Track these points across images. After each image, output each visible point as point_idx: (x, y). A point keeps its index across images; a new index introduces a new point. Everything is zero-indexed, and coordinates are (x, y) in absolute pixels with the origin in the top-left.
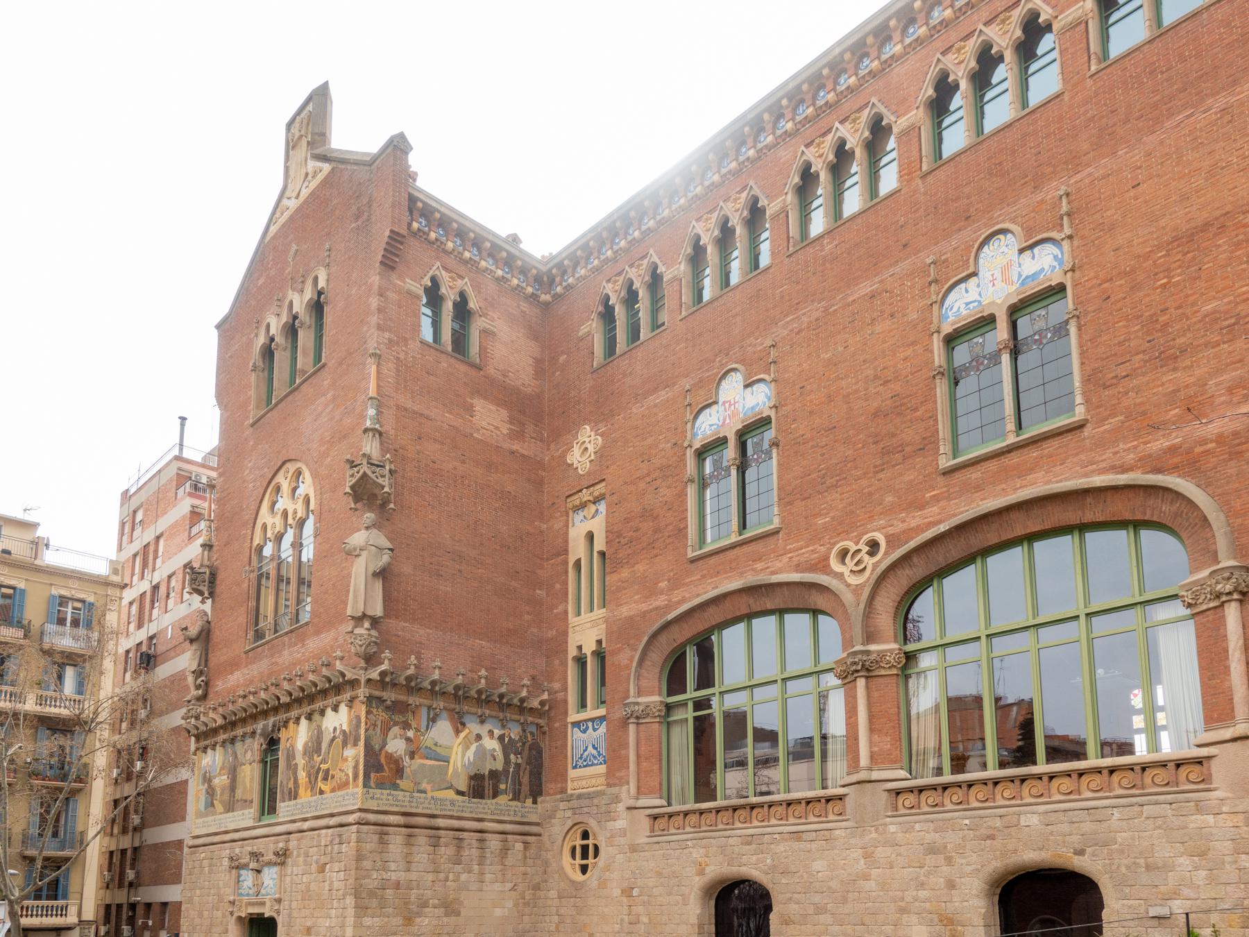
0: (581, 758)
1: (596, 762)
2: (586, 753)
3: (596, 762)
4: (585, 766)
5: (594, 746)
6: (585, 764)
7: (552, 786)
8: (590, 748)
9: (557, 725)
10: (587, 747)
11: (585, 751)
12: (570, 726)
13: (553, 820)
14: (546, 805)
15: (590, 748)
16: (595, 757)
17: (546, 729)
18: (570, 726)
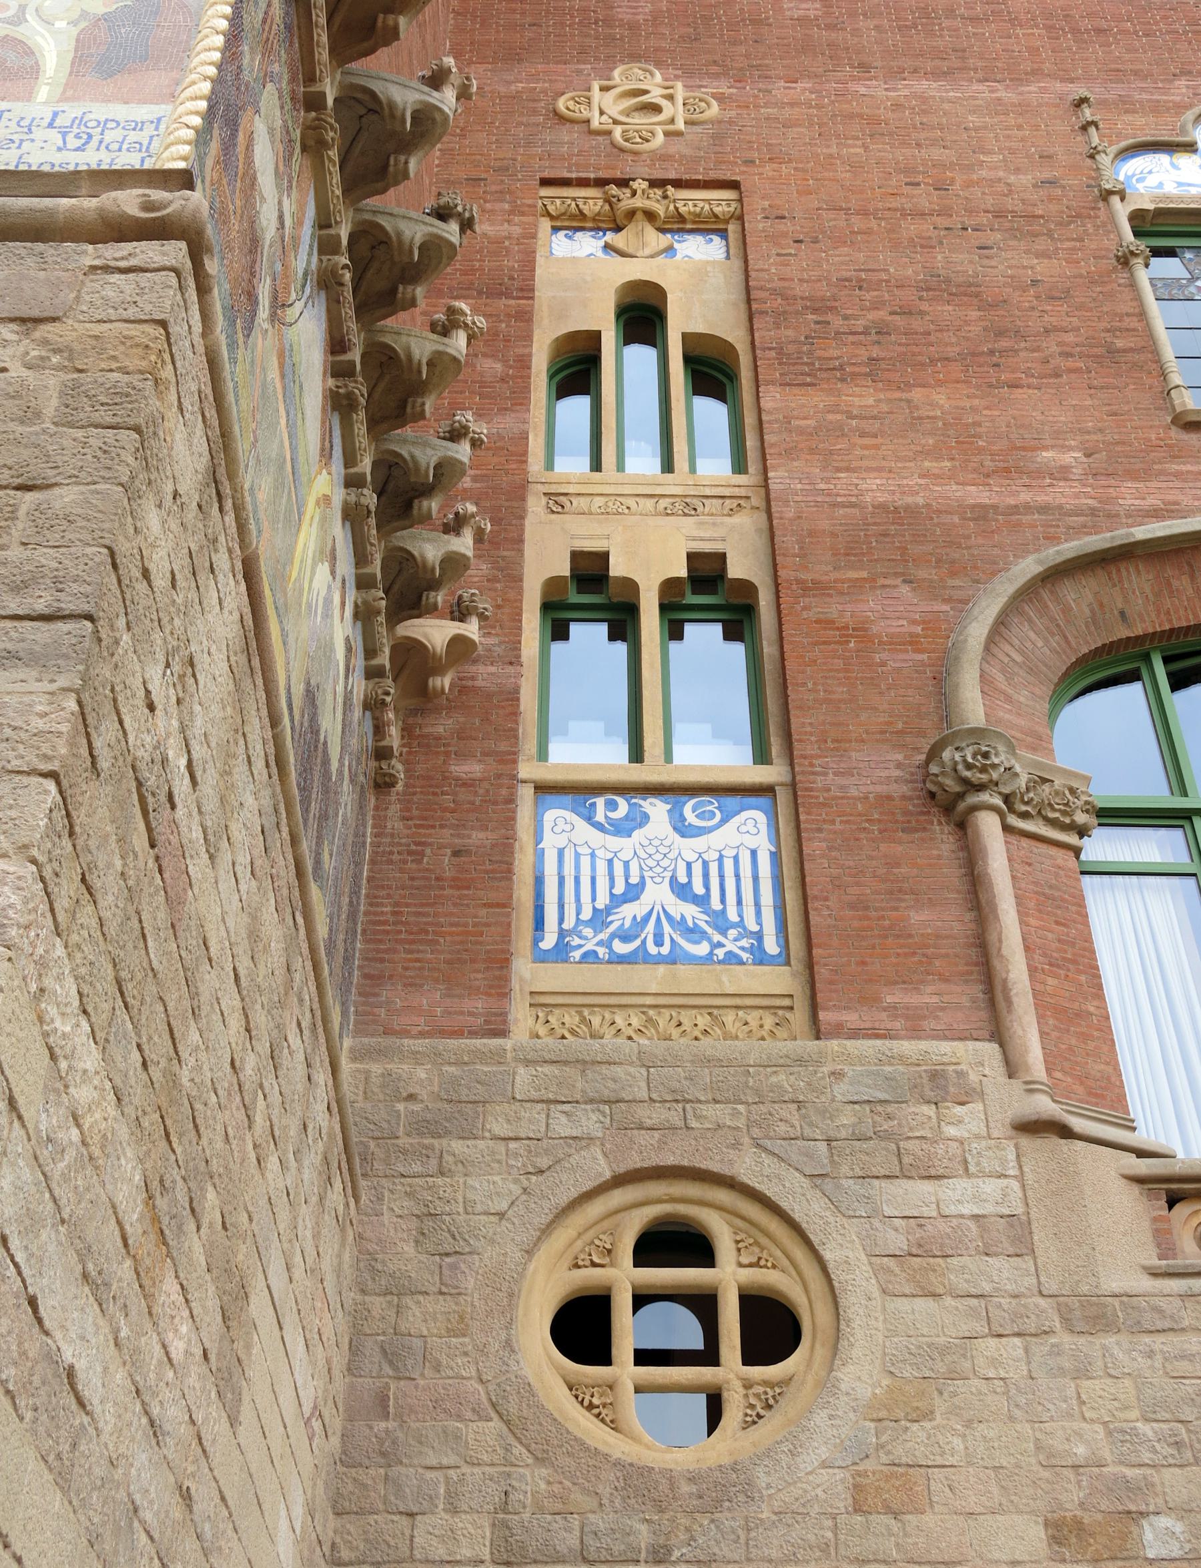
0: (600, 918)
1: (702, 949)
2: (628, 912)
3: (702, 949)
4: (622, 960)
5: (682, 891)
6: (621, 948)
7: (431, 998)
8: (658, 894)
9: (471, 769)
10: (633, 892)
11: (617, 901)
12: (526, 794)
13: (457, 1146)
14: (402, 1068)
15: (658, 894)
16: (693, 932)
17: (398, 768)
18: (526, 794)
